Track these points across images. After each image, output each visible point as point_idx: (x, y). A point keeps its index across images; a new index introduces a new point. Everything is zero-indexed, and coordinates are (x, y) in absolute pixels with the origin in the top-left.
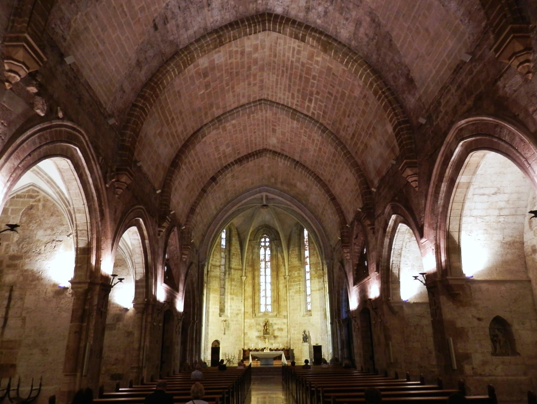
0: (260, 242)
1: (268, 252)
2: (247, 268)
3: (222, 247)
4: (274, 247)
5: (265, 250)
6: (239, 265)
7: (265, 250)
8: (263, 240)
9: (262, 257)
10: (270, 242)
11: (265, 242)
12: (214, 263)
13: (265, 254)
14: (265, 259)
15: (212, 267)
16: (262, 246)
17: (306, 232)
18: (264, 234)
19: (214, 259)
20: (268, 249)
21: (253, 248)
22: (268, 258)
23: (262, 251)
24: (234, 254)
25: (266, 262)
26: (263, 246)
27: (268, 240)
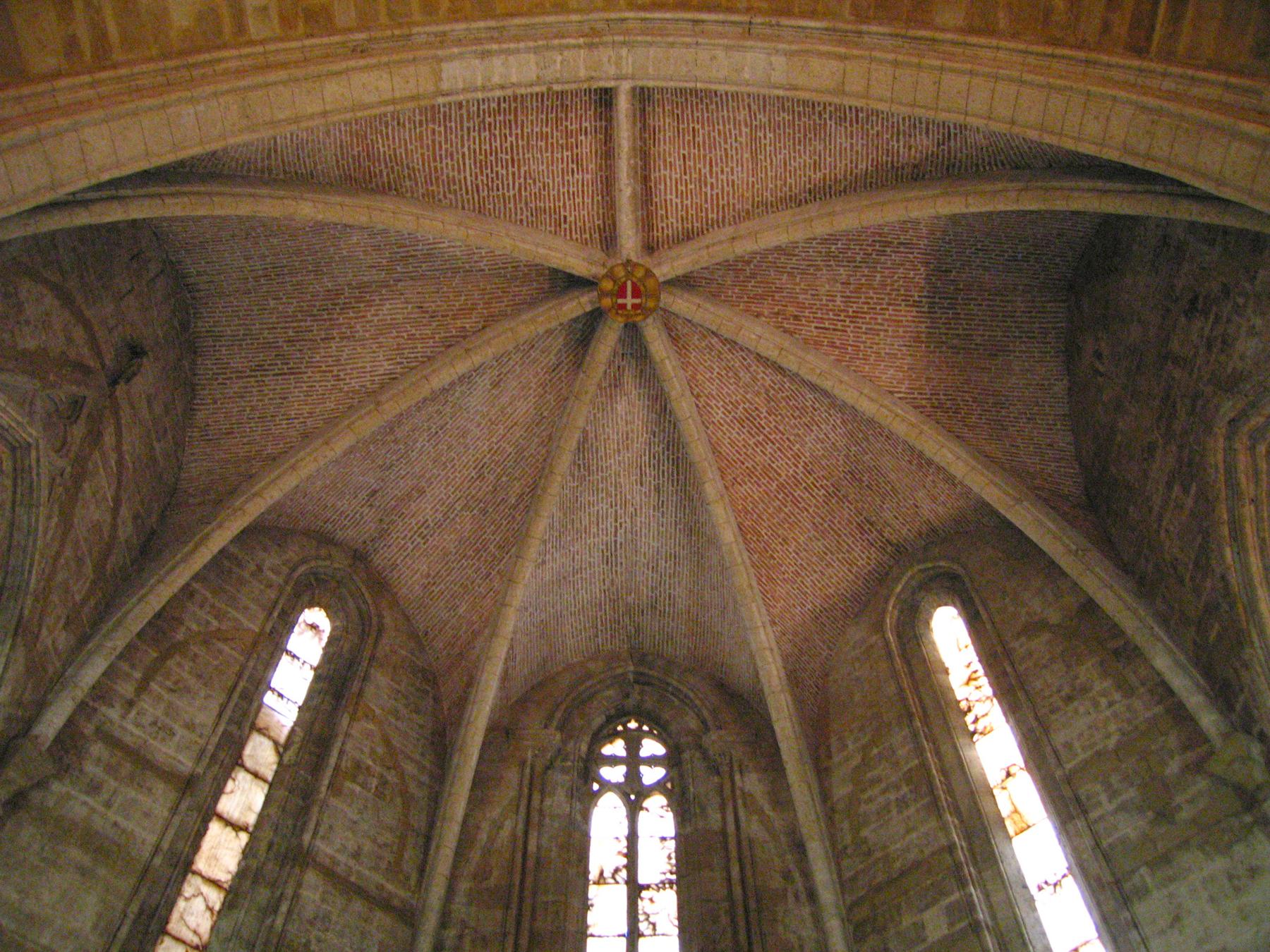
0: (593, 760)
1: (658, 819)
2: (460, 907)
3: (269, 698)
4: (702, 786)
5: (634, 809)
6: (394, 869)
7: (634, 809)
8: (617, 748)
9: (604, 851)
10: (671, 761)
11: (633, 761)
12: (132, 730)
13: (632, 838)
14: (632, 866)
15: (97, 749)
16: (606, 786)
17: (949, 632)
18: (623, 714)
19: (150, 708)
20: (656, 803)
21: (536, 784)
22: (657, 861)
23: (607, 817)
24: (358, 765)
25: (635, 890)
26: (617, 787)
27: (652, 747)
